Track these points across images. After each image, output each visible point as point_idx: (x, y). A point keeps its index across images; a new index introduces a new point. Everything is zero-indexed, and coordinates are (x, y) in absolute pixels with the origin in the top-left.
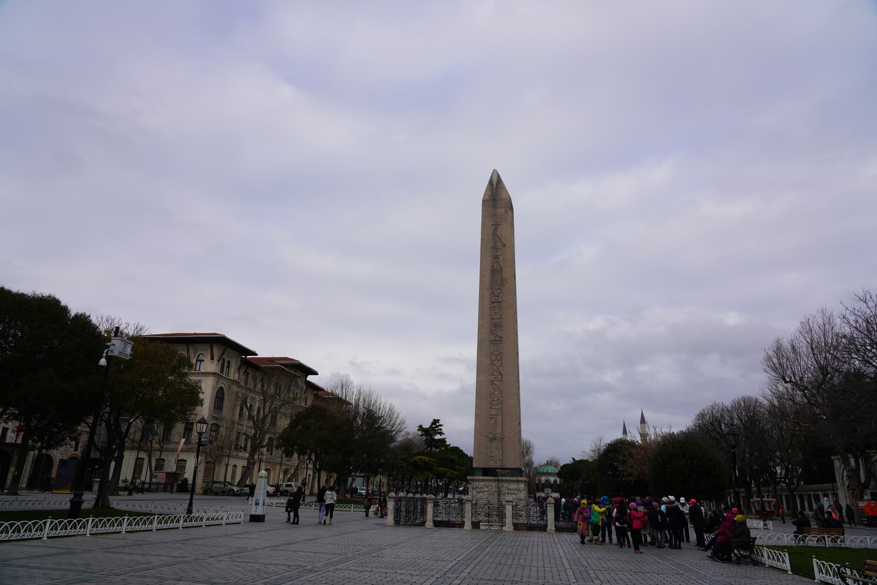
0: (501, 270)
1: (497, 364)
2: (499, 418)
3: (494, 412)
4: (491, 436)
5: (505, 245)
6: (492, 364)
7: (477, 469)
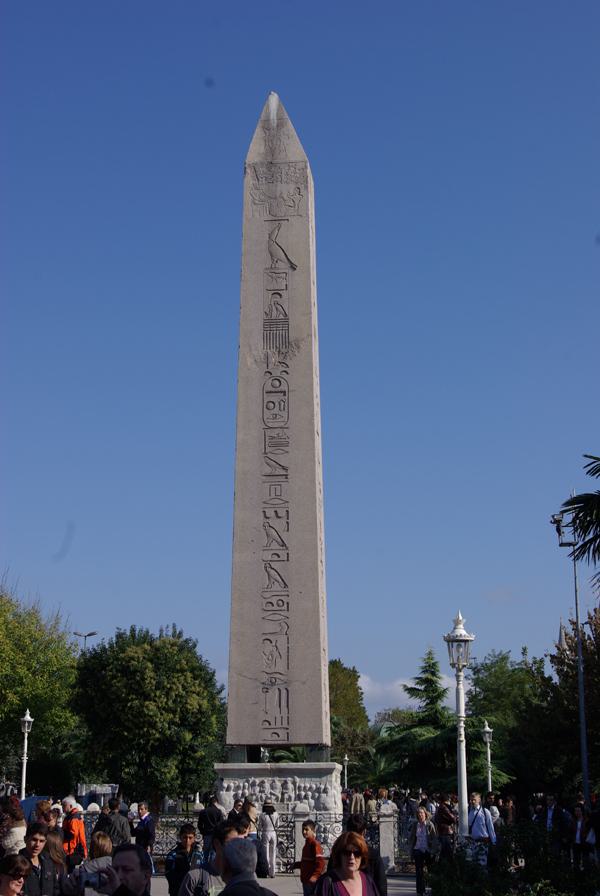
1: (274, 522)
3: (270, 627)
4: (265, 678)
5: (293, 267)
6: (268, 527)
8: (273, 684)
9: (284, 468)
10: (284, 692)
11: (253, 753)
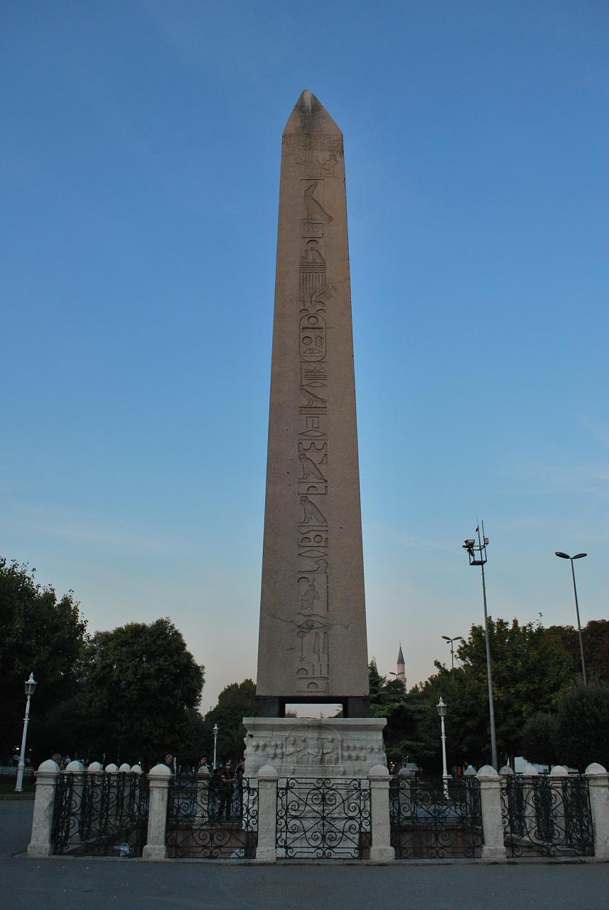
0: (323, 265)
2: (321, 578)
3: (308, 565)
4: (301, 620)
5: (331, 219)
6: (303, 457)
7: (265, 698)
8: (311, 628)
9: (323, 401)
10: (322, 636)
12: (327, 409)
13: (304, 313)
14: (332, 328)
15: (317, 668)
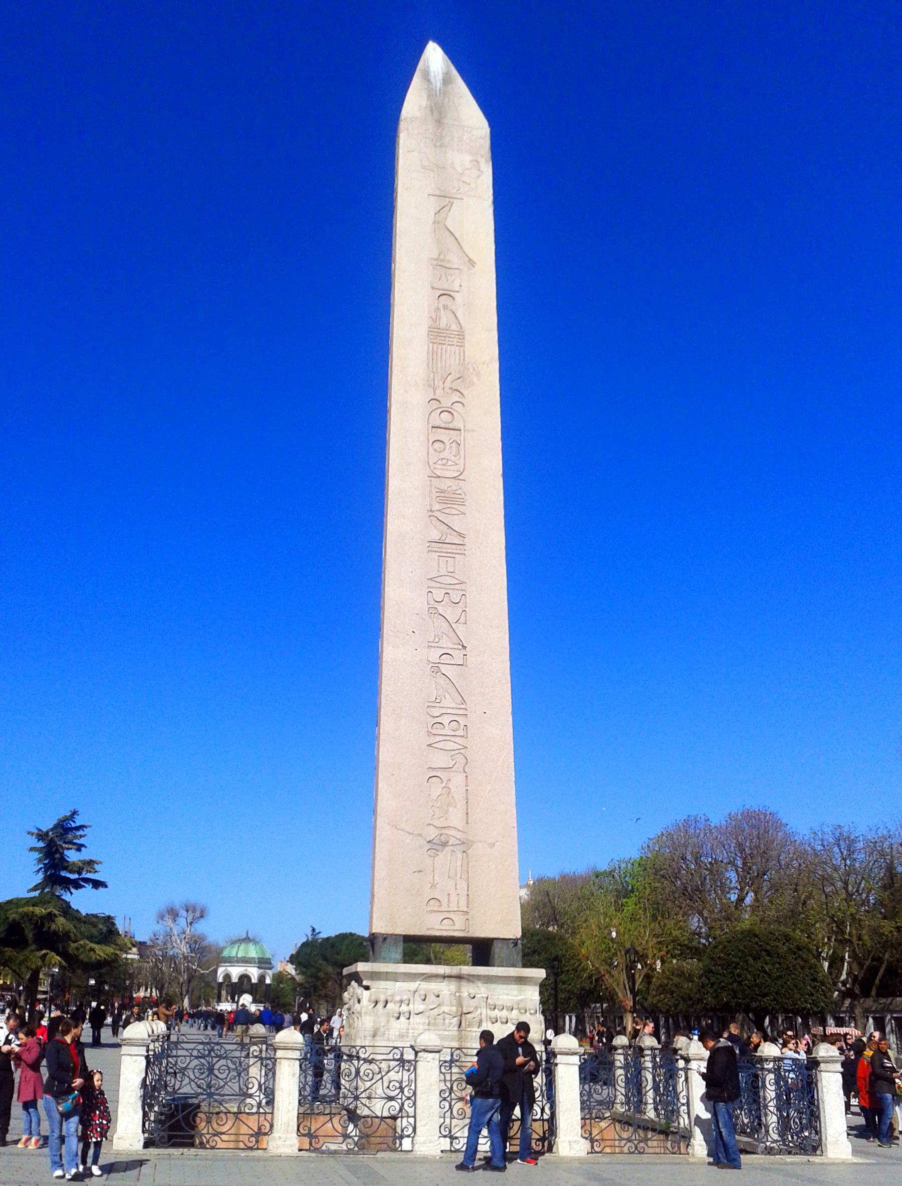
0: (461, 335)
2: (457, 780)
3: (441, 760)
4: (432, 833)
6: (433, 611)
8: (445, 844)
9: (460, 535)
10: (460, 855)
11: (418, 948)
12: (465, 548)
13: (435, 404)
14: (473, 431)
15: (454, 899)
